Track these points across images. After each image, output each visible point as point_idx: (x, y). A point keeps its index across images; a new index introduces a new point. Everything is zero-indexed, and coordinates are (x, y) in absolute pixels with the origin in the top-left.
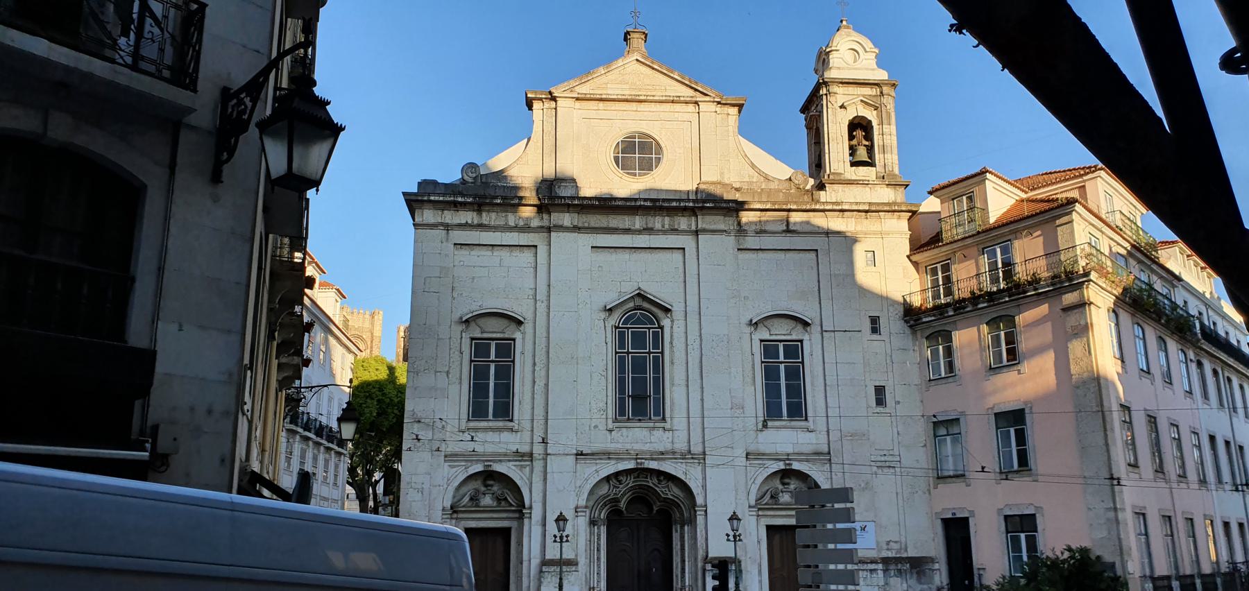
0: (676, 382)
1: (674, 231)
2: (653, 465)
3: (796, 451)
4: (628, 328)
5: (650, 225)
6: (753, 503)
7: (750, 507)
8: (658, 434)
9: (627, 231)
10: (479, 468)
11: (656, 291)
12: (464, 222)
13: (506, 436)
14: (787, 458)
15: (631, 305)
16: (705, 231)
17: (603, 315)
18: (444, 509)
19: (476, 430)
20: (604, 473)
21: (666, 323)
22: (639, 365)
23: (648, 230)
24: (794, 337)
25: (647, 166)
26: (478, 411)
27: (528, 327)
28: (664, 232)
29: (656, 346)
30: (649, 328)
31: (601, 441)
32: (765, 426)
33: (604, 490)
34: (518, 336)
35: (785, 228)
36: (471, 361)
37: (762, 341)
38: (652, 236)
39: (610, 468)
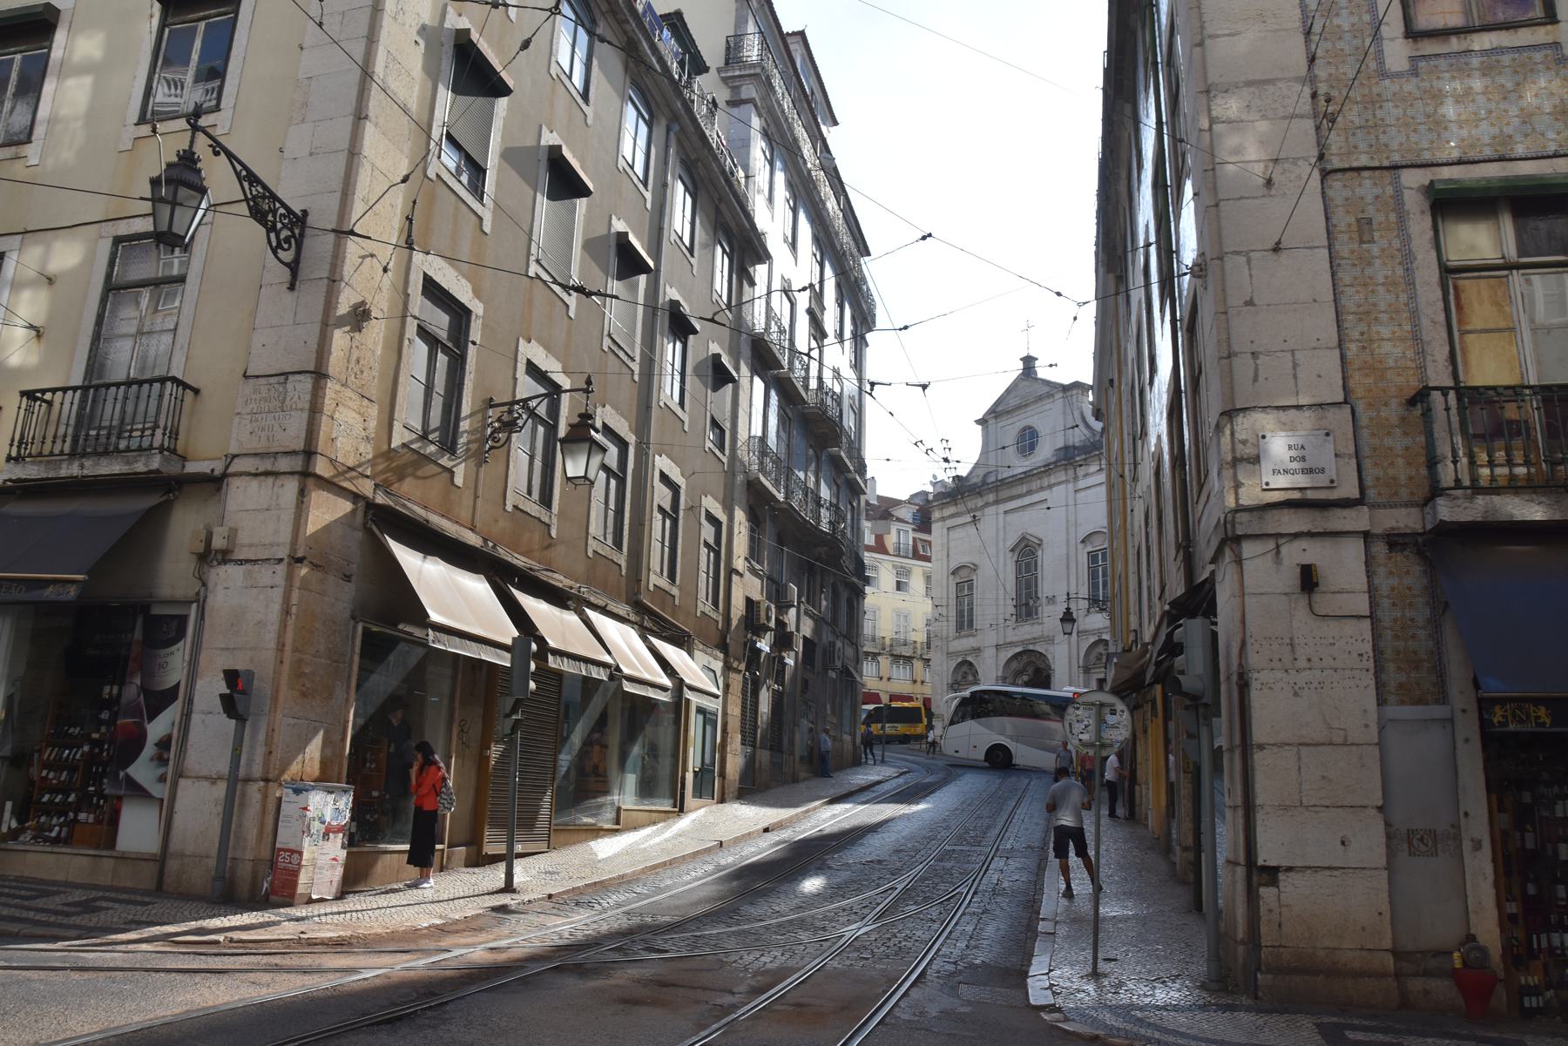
1: (1042, 489)
2: (1031, 647)
8: (1036, 626)
9: (1020, 496)
11: (1035, 530)
13: (971, 639)
14: (1099, 631)
15: (1022, 545)
16: (1054, 485)
17: (1011, 554)
20: (1009, 655)
21: (1040, 553)
22: (1028, 586)
23: (1030, 492)
25: (1032, 447)
26: (960, 627)
27: (978, 571)
28: (1037, 491)
29: (1036, 570)
31: (1012, 636)
32: (1088, 612)
33: (1014, 665)
34: (974, 578)
37: (1089, 553)
39: (1010, 653)
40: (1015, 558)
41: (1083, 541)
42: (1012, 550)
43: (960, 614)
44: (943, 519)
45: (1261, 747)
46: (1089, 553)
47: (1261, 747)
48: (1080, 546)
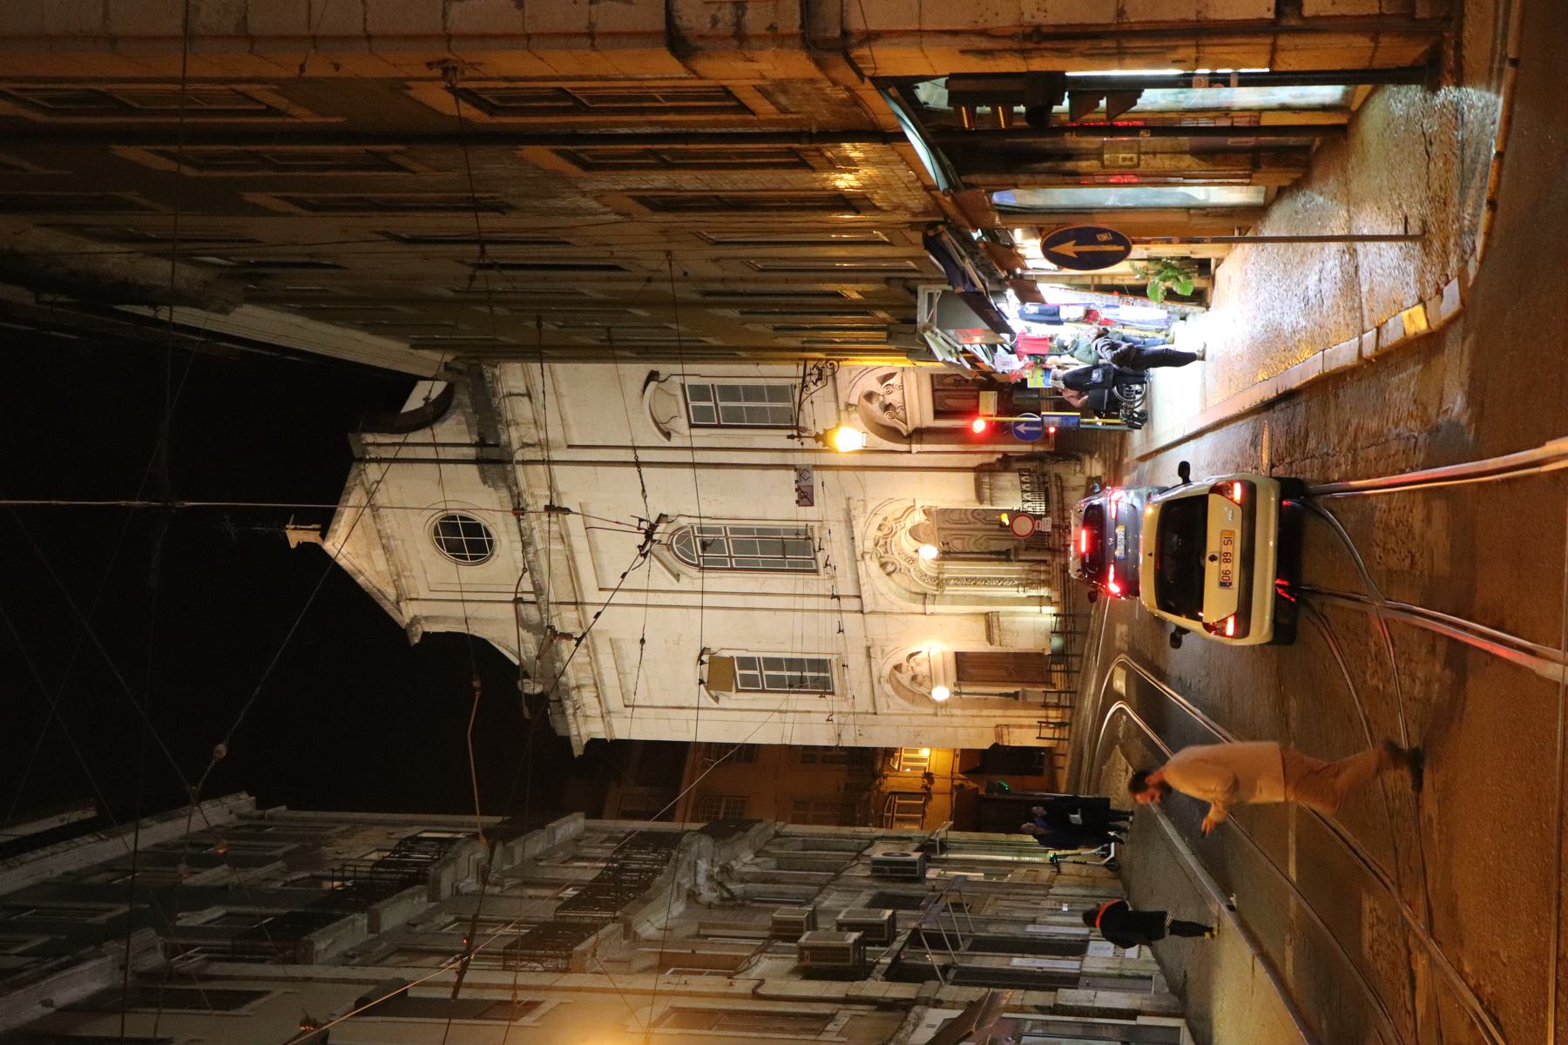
0: (759, 515)
3: (833, 399)
4: (699, 556)
5: (558, 536)
6: (904, 447)
7: (910, 452)
9: (571, 558)
10: (888, 688)
12: (596, 699)
18: (936, 715)
19: (844, 688)
24: (679, 393)
25: (474, 529)
26: (823, 687)
29: (718, 531)
30: (695, 537)
35: (526, 400)
36: (763, 691)
37: (692, 426)
38: (572, 533)
40: (694, 572)
41: (668, 435)
42: (677, 577)
43: (798, 685)
44: (606, 714)
45: (1121, 12)
46: (692, 426)
47: (1121, 12)
48: (676, 441)
